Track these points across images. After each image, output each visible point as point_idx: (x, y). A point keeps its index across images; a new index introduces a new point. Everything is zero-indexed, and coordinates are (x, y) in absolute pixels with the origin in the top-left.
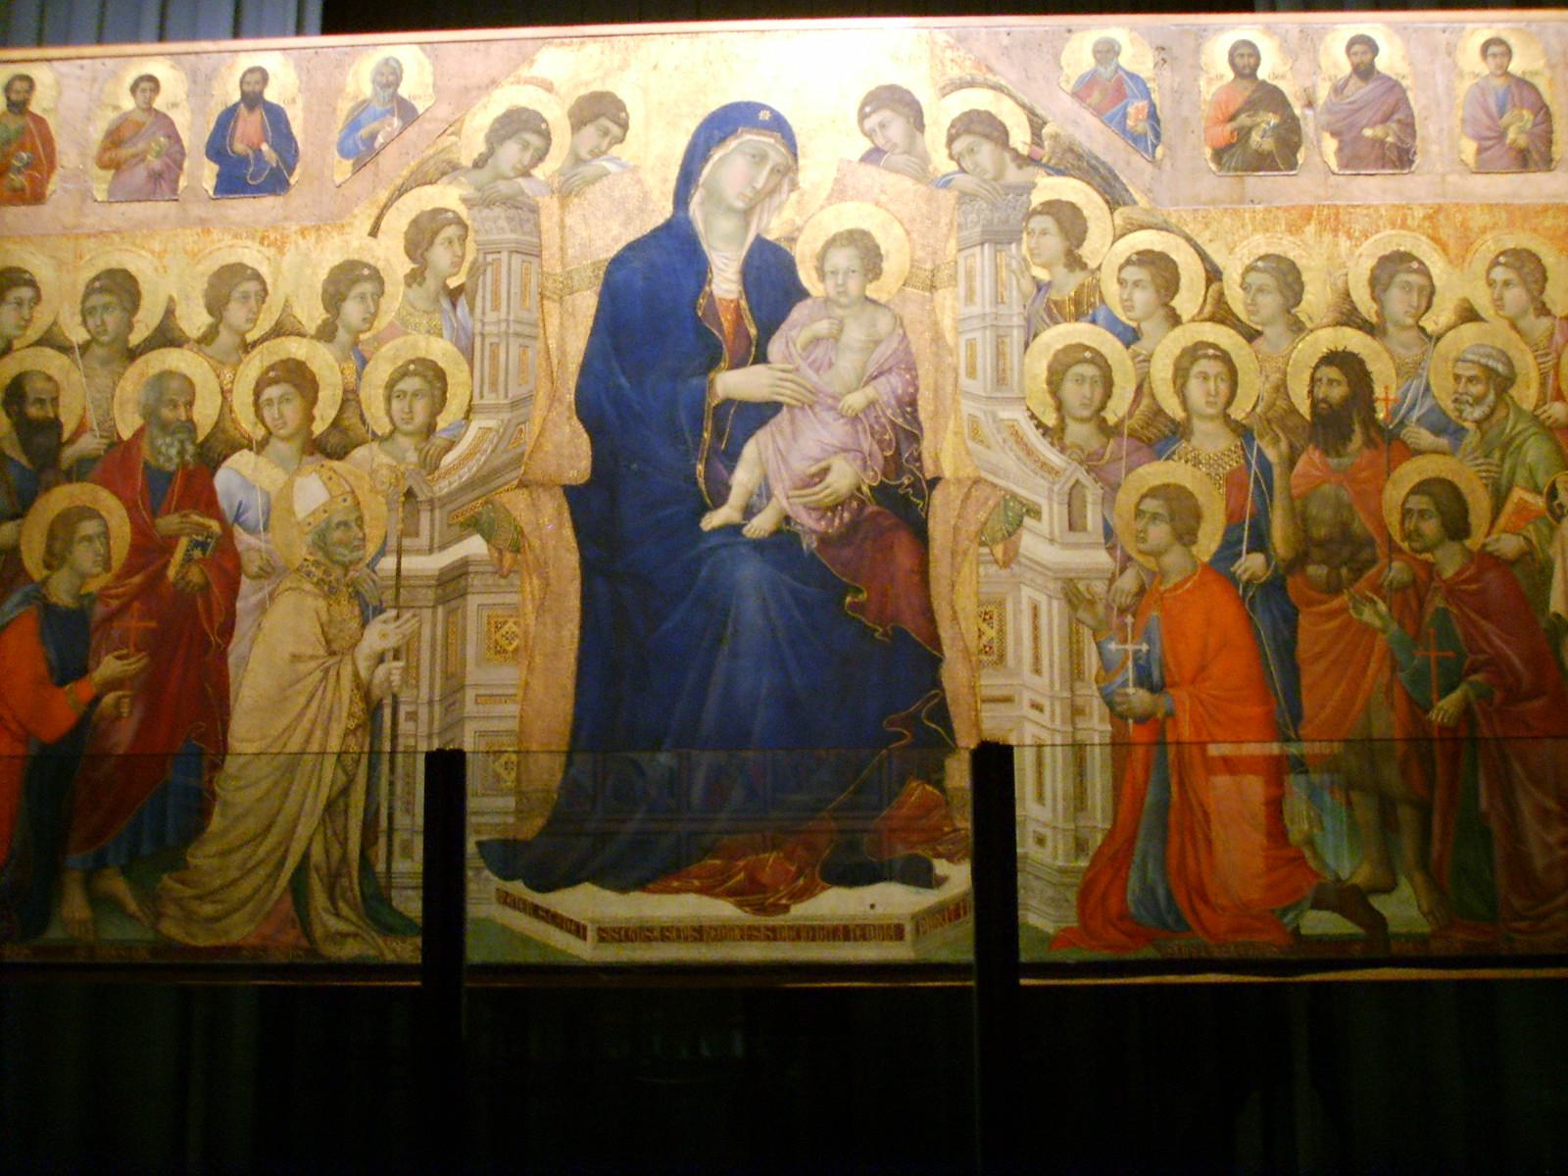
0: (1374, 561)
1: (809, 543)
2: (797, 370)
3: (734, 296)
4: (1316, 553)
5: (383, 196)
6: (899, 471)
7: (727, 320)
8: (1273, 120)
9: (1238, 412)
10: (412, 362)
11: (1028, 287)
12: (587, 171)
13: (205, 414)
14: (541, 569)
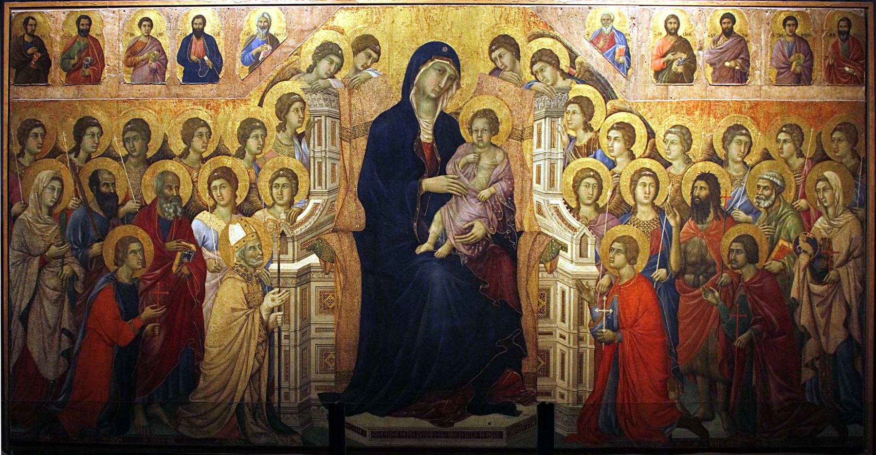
0: (715, 273)
1: (464, 260)
2: (459, 178)
3: (430, 141)
4: (689, 269)
5: (264, 86)
6: (505, 229)
7: (427, 154)
8: (684, 56)
9: (658, 203)
10: (281, 170)
11: (565, 139)
12: (362, 76)
13: (185, 192)
14: (344, 271)
